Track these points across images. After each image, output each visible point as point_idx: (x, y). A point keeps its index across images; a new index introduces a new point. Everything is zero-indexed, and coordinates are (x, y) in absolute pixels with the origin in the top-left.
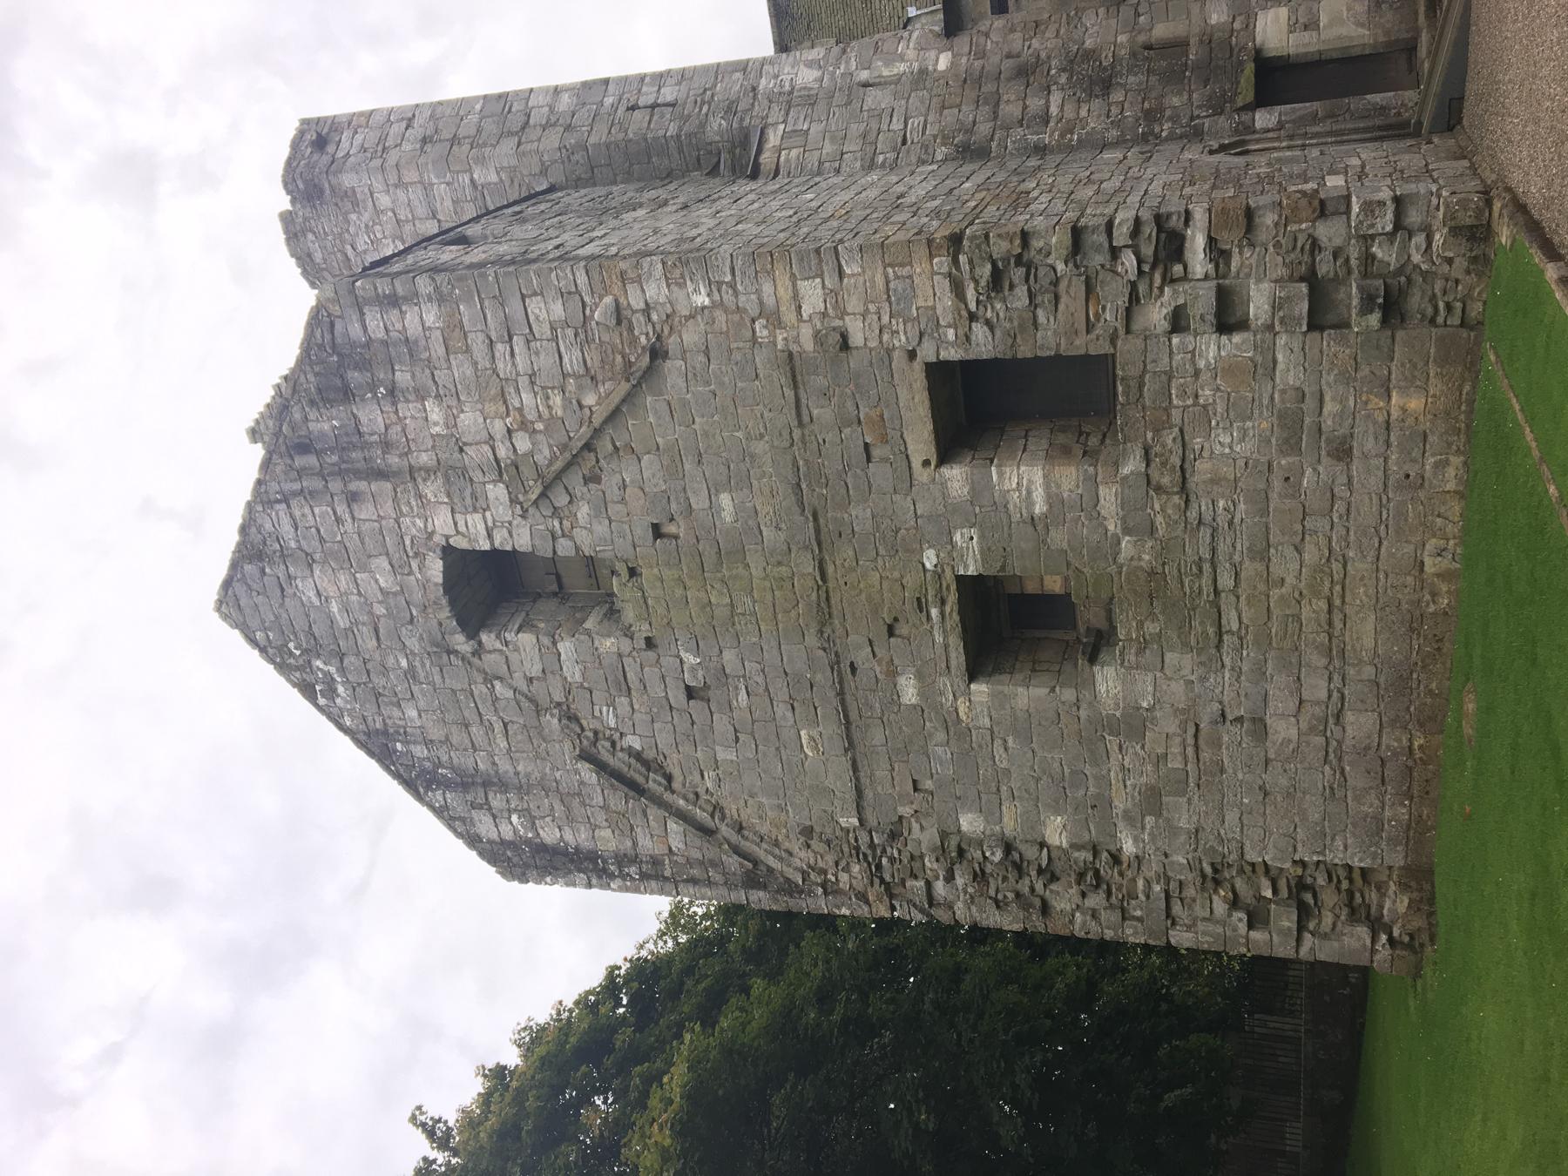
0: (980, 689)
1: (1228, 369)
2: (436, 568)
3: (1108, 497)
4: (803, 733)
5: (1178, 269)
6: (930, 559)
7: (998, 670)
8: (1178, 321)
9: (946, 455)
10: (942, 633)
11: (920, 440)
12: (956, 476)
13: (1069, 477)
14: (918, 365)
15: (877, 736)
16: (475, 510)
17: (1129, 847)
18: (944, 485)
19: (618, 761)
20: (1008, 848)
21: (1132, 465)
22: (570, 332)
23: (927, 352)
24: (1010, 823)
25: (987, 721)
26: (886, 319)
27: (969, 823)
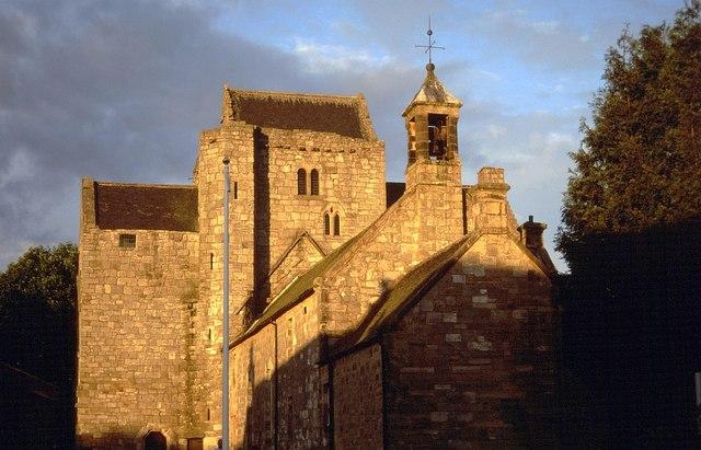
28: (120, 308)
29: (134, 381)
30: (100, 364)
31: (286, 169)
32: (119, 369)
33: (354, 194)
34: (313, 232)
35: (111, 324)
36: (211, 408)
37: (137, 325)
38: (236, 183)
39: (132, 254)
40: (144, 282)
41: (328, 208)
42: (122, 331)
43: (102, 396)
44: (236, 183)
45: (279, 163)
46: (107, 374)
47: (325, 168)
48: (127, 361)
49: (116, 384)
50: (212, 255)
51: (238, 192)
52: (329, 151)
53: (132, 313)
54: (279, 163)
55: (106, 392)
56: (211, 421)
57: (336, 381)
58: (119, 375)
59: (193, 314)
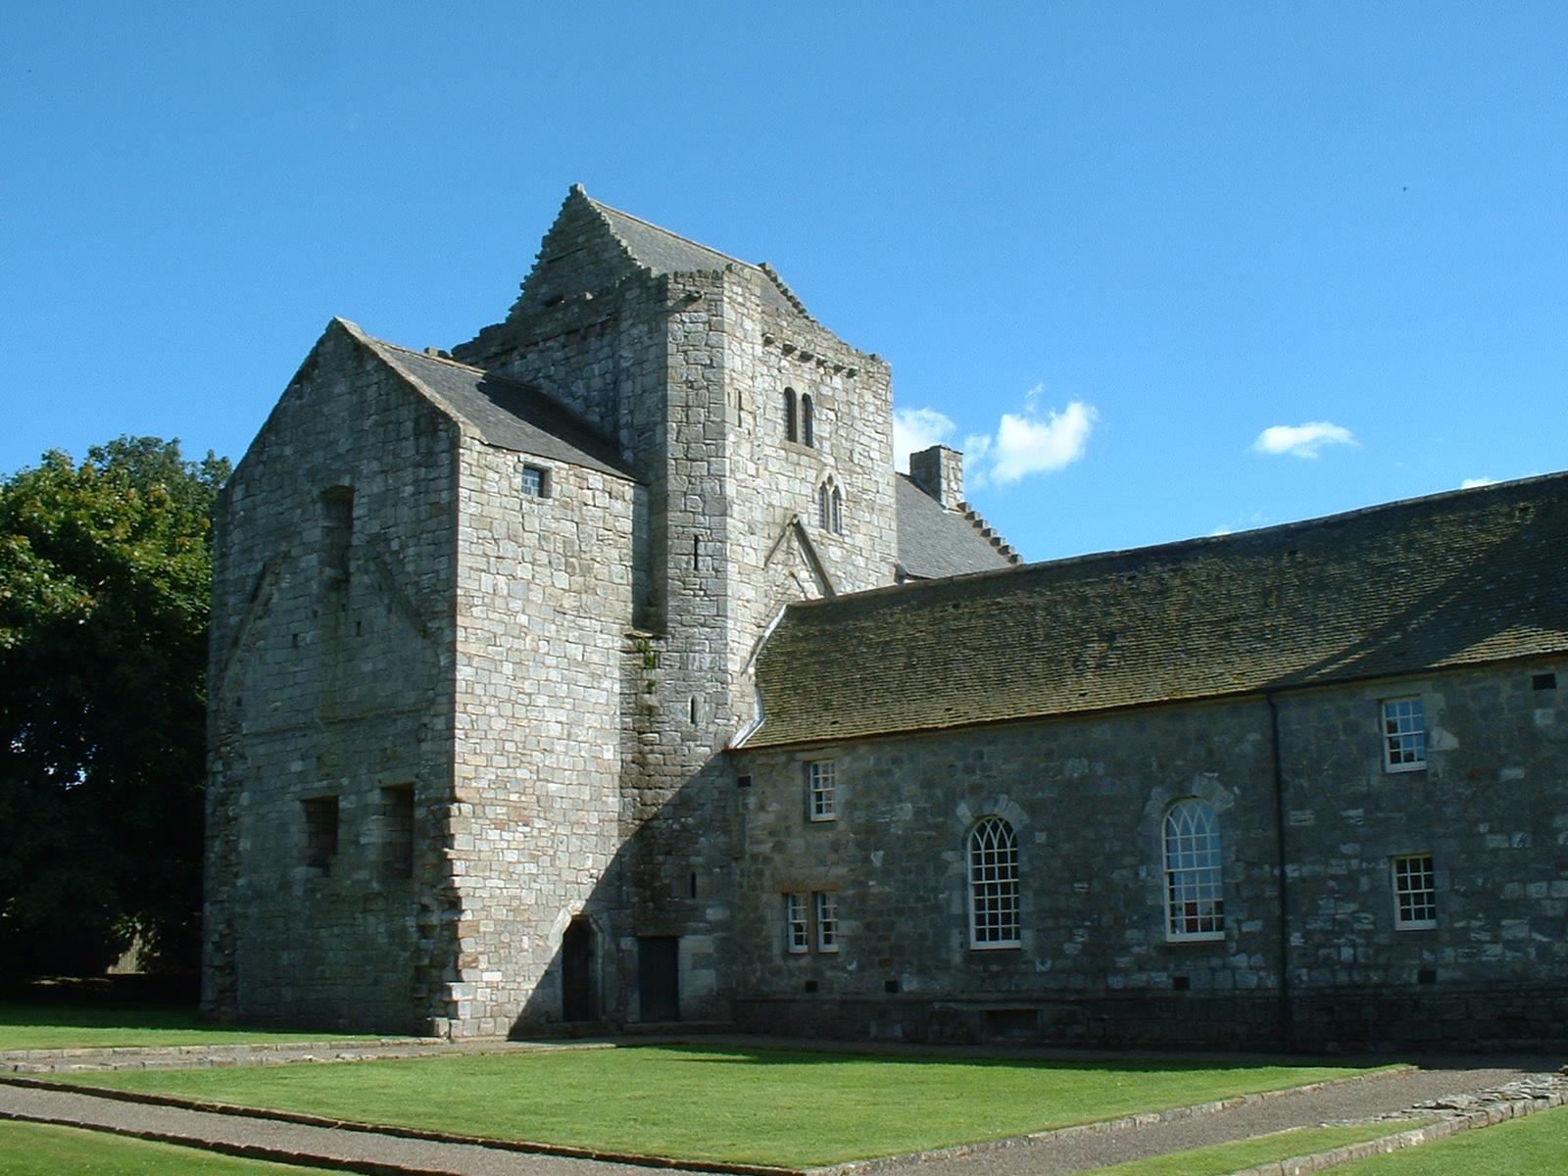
0: (297, 806)
1: (404, 930)
2: (346, 481)
3: (363, 875)
4: (278, 704)
5: (447, 906)
6: (345, 782)
7: (309, 815)
8: (425, 908)
9: (386, 790)
10: (318, 786)
11: (389, 778)
12: (375, 797)
13: (372, 856)
14: (414, 779)
15: (278, 746)
16: (369, 510)
17: (241, 882)
18: (371, 790)
19: (266, 589)
20: (235, 819)
21: (376, 886)
22: (434, 581)
23: (419, 784)
24: (247, 820)
25: (285, 809)
26: (430, 763)
27: (245, 798)
28: (524, 631)
30: (489, 758)
32: (522, 773)
35: (508, 668)
36: (699, 871)
37: (554, 675)
39: (544, 515)
40: (562, 580)
43: (494, 834)
46: (501, 783)
49: (516, 807)
55: (500, 826)
56: (699, 901)
59: (651, 663)
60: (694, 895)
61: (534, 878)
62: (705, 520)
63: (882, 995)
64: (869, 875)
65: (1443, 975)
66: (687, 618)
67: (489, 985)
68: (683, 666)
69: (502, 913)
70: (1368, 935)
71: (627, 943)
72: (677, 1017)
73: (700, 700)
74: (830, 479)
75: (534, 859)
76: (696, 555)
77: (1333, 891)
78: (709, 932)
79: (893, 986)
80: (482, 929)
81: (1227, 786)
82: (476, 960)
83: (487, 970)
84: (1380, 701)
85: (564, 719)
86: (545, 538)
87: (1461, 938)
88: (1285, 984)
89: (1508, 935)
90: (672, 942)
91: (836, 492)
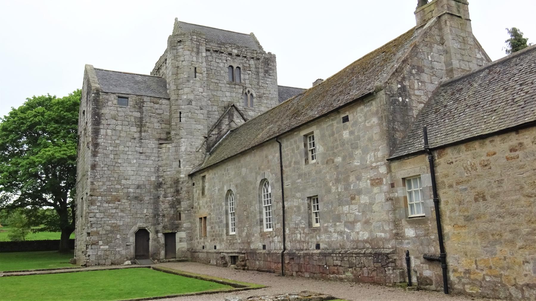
29: (128, 196)
30: (104, 184)
31: (221, 65)
33: (260, 84)
34: (238, 104)
37: (130, 157)
38: (195, 68)
41: (247, 91)
42: (119, 161)
44: (195, 68)
45: (217, 61)
47: (244, 66)
48: (123, 182)
50: (180, 113)
51: (197, 74)
52: (245, 57)
53: (126, 149)
54: (217, 61)
57: (452, 276)
58: (117, 190)
60: (180, 219)
61: (122, 217)
62: (183, 107)
63: (214, 250)
64: (211, 211)
65: (322, 246)
66: (178, 137)
67: (102, 250)
68: (177, 151)
69: (109, 228)
70: (303, 229)
71: (160, 235)
72: (175, 258)
73: (181, 160)
74: (249, 91)
75: (122, 211)
76: (180, 118)
77: (295, 212)
78: (184, 231)
79: (215, 248)
80: (100, 233)
81: (272, 174)
82: (98, 242)
83: (102, 245)
84: (306, 136)
85: (135, 170)
86: (127, 117)
87: (326, 231)
88: (285, 249)
89: (338, 229)
90: (174, 234)
91: (252, 95)
